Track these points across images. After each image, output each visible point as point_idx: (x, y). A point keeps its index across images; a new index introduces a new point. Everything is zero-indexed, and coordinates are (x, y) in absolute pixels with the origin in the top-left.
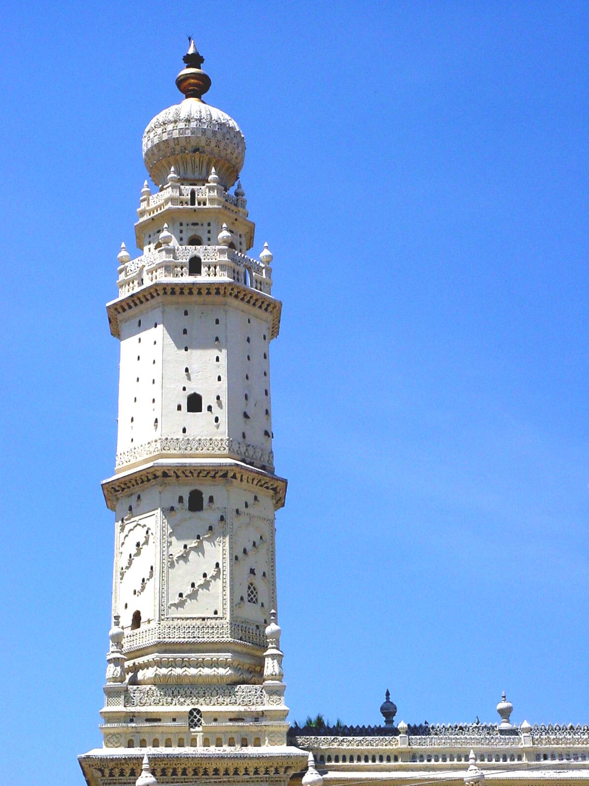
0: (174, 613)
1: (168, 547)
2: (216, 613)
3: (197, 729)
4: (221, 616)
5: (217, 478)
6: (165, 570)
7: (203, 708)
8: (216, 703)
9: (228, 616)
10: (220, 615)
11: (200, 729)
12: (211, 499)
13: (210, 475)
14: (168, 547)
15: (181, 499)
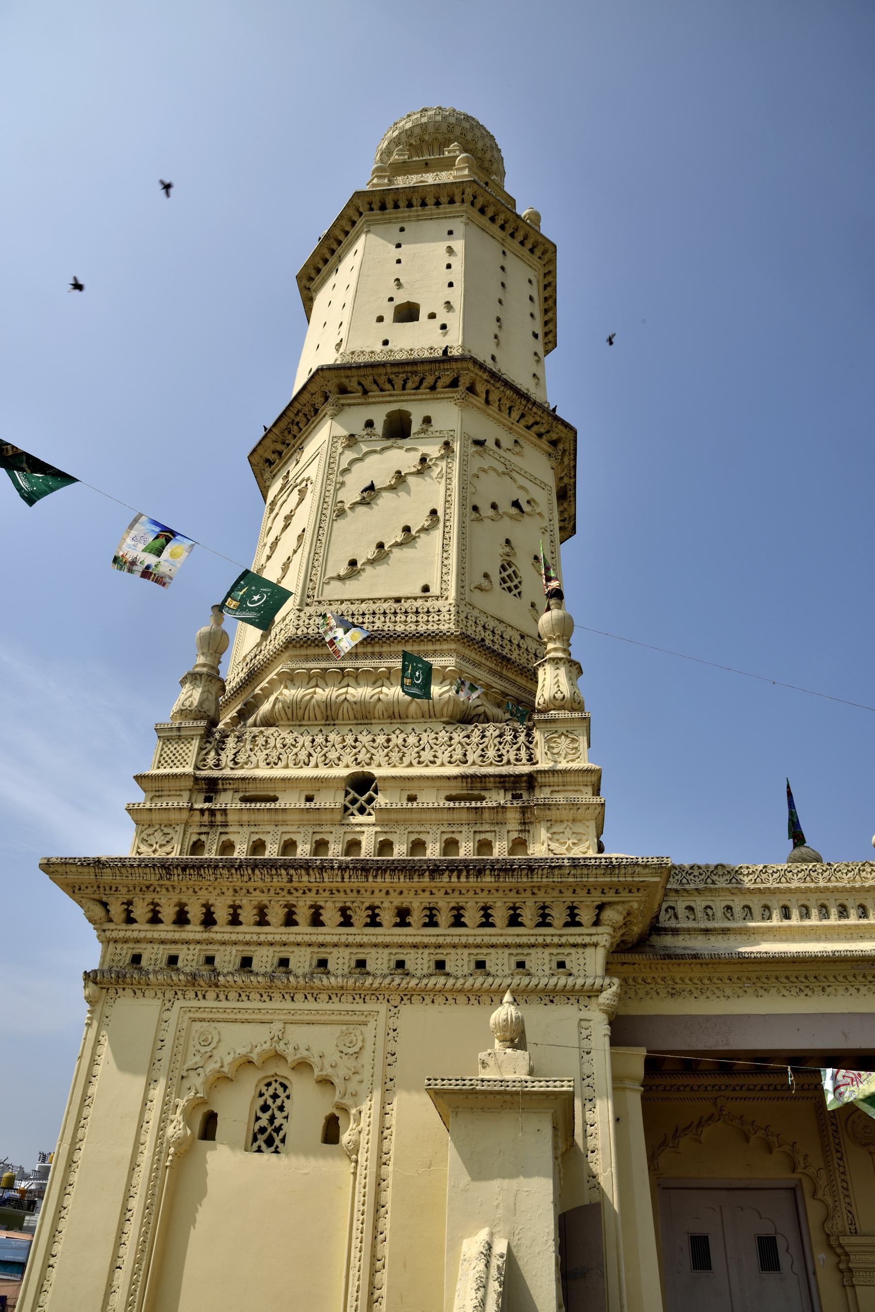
0: (335, 590)
1: (336, 490)
2: (426, 589)
3: (360, 819)
4: (438, 593)
5: (439, 390)
6: (325, 525)
7: (377, 772)
8: (415, 762)
9: (452, 594)
10: (435, 590)
11: (372, 819)
12: (427, 420)
13: (425, 384)
14: (336, 490)
15: (370, 424)
